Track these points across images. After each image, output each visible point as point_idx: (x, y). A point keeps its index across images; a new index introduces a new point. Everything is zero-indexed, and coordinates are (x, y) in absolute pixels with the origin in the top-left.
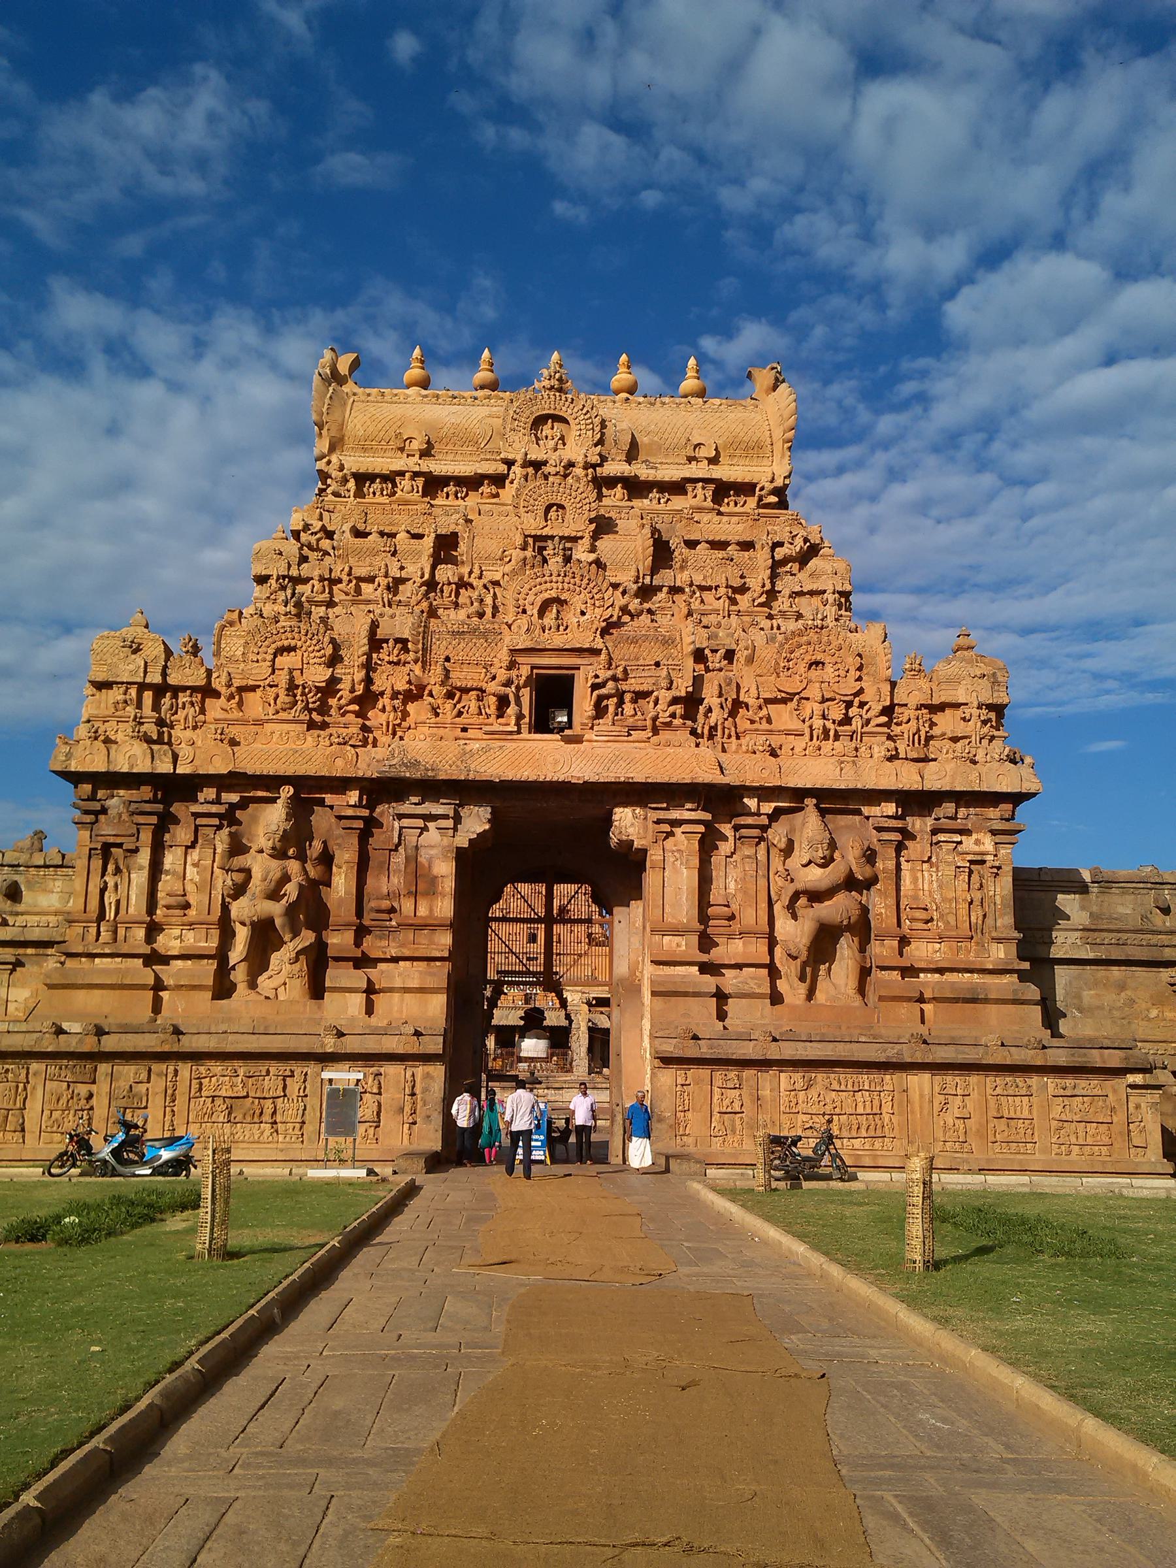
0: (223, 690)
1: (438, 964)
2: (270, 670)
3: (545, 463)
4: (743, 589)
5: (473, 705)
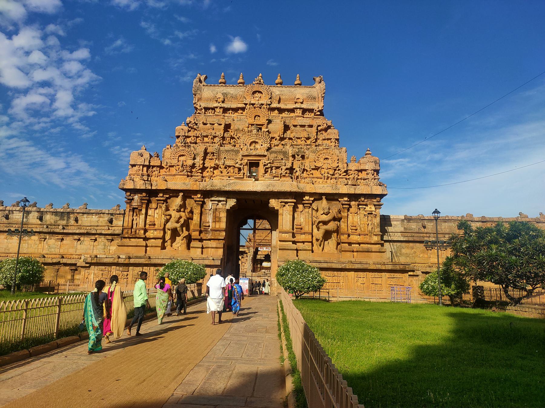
0: (165, 167)
1: (221, 241)
2: (177, 161)
3: (255, 104)
4: (308, 138)
5: (232, 171)
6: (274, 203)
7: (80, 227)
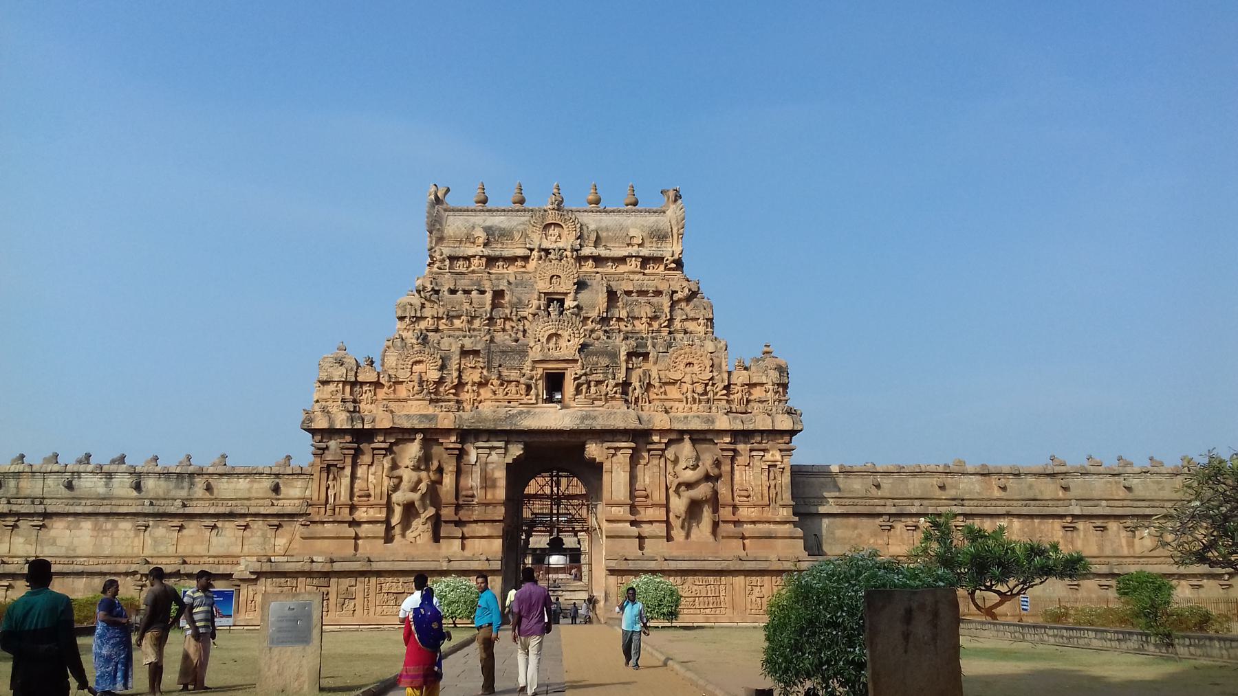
0: (387, 384)
1: (498, 523)
2: (410, 373)
4: (655, 318)
6: (593, 450)
7: (215, 501)
